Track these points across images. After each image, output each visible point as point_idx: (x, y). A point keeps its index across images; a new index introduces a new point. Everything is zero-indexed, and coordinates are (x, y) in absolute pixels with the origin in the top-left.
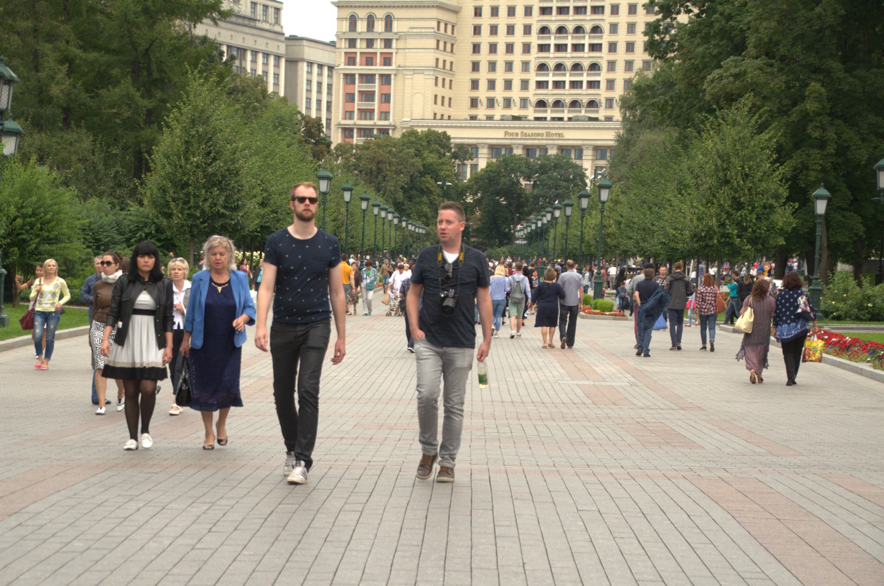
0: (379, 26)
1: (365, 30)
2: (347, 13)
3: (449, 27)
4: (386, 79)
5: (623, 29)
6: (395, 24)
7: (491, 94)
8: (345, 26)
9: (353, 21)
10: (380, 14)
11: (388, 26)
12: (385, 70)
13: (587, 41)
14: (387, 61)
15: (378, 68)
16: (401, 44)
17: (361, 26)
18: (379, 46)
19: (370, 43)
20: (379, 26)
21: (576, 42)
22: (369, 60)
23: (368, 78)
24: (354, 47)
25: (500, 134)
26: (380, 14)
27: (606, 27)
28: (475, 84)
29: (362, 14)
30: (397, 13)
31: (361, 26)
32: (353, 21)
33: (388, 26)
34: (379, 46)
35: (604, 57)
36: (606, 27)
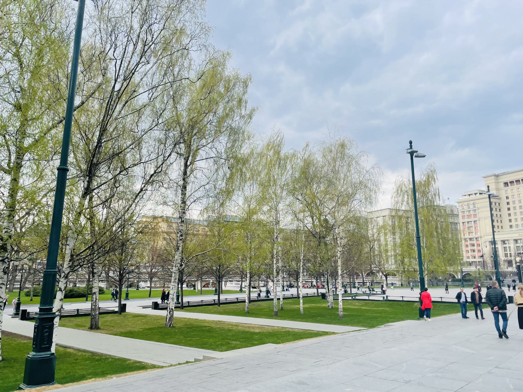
0: (471, 207)
3: (497, 204)
6: (476, 205)
7: (517, 223)
11: (475, 207)
12: (475, 219)
14: (475, 215)
15: (473, 219)
16: (479, 211)
18: (472, 213)
20: (471, 207)
22: (469, 216)
25: (517, 235)
28: (510, 221)
33: (475, 207)
34: (472, 213)
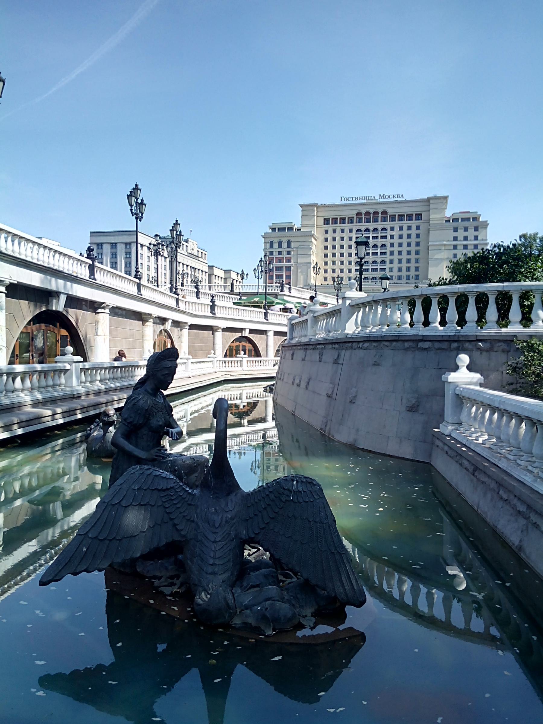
0: (285, 245)
1: (277, 247)
2: (269, 240)
4: (288, 269)
5: (396, 245)
8: (268, 245)
9: (272, 244)
10: (285, 240)
11: (289, 246)
12: (288, 264)
13: (379, 251)
15: (285, 264)
17: (276, 245)
18: (284, 255)
19: (280, 253)
20: (285, 245)
21: (373, 251)
22: (280, 260)
23: (279, 268)
24: (272, 255)
26: (285, 240)
27: (388, 245)
29: (276, 240)
30: (292, 239)
31: (276, 245)
32: (272, 244)
33: (289, 246)
34: (284, 255)
35: (387, 258)
36: (388, 245)
